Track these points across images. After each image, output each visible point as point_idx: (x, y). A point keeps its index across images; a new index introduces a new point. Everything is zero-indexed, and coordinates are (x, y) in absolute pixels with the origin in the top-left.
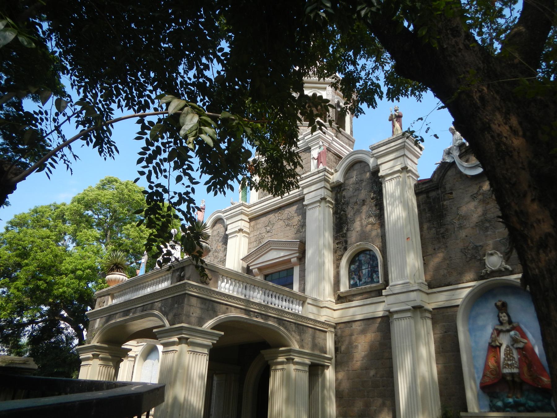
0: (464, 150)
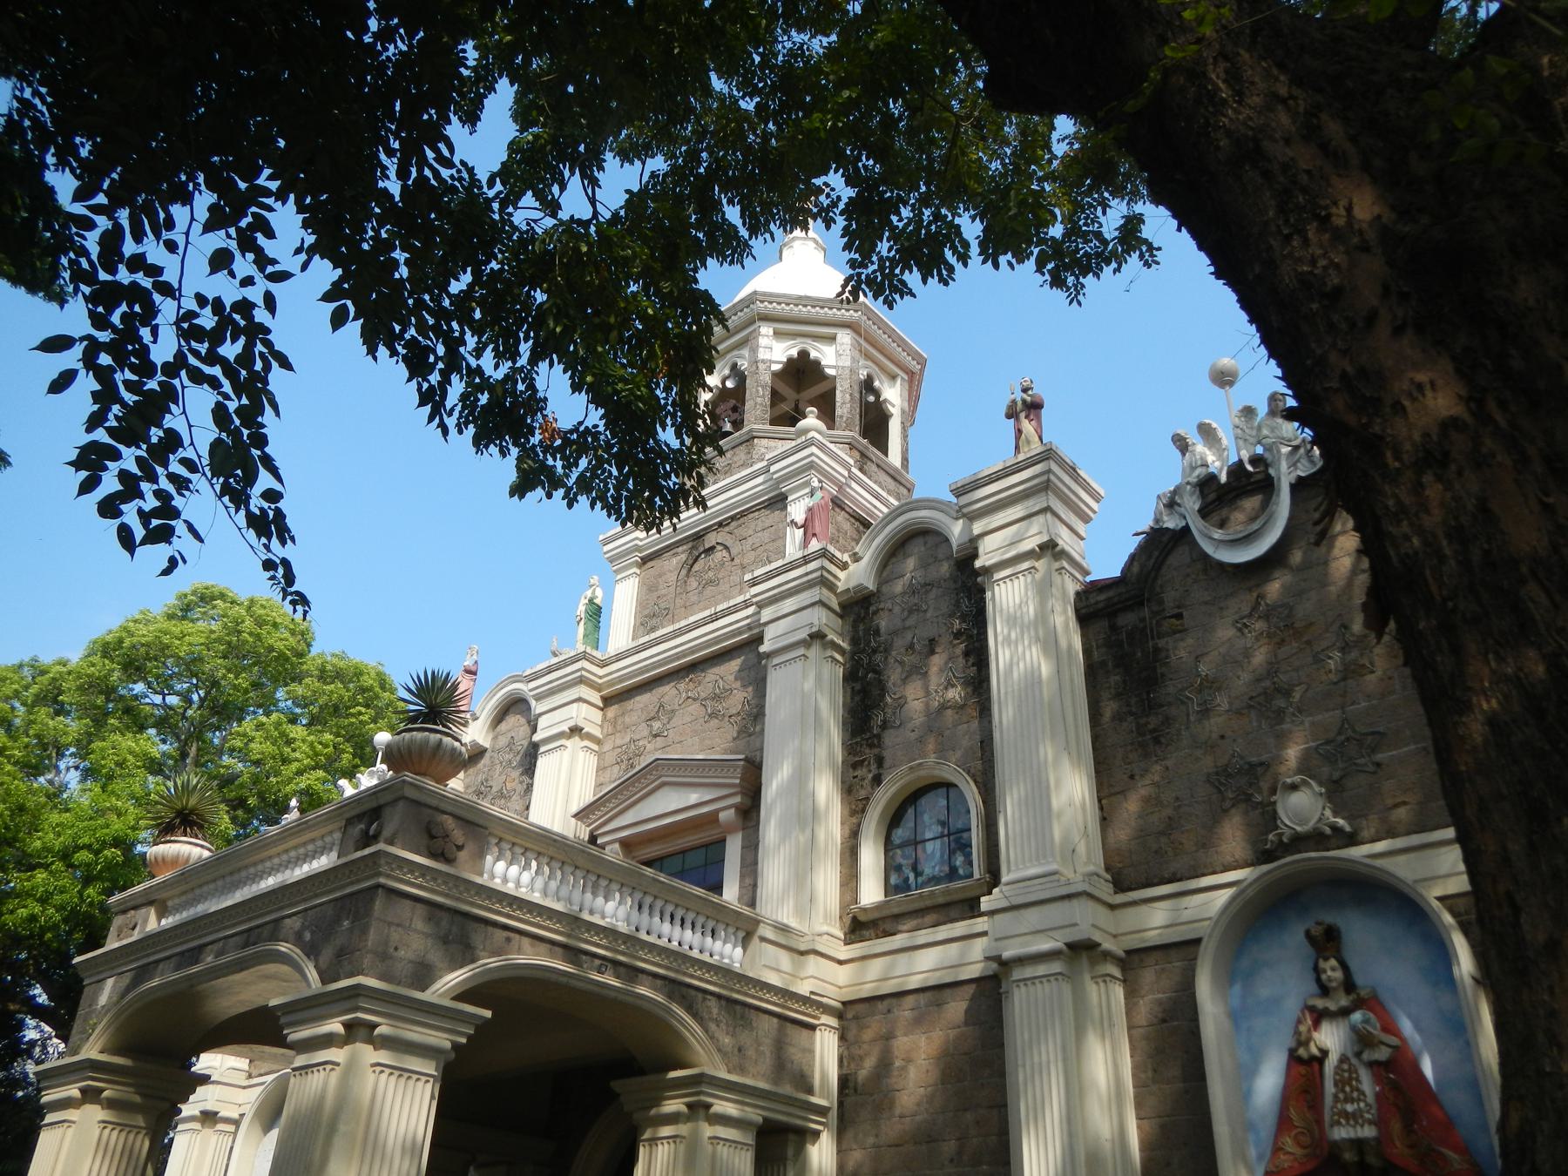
0: (1212, 496)
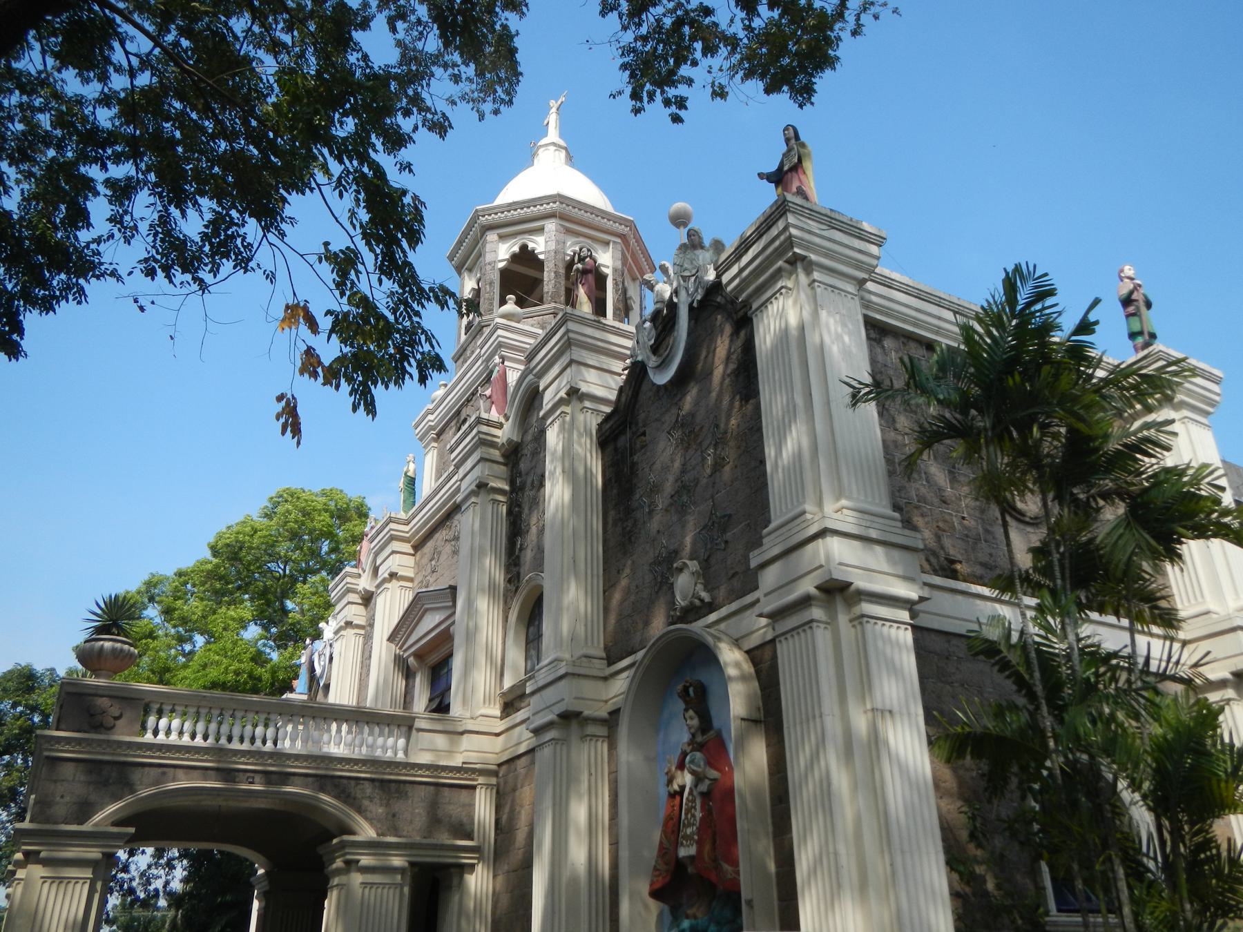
0: (660, 328)
